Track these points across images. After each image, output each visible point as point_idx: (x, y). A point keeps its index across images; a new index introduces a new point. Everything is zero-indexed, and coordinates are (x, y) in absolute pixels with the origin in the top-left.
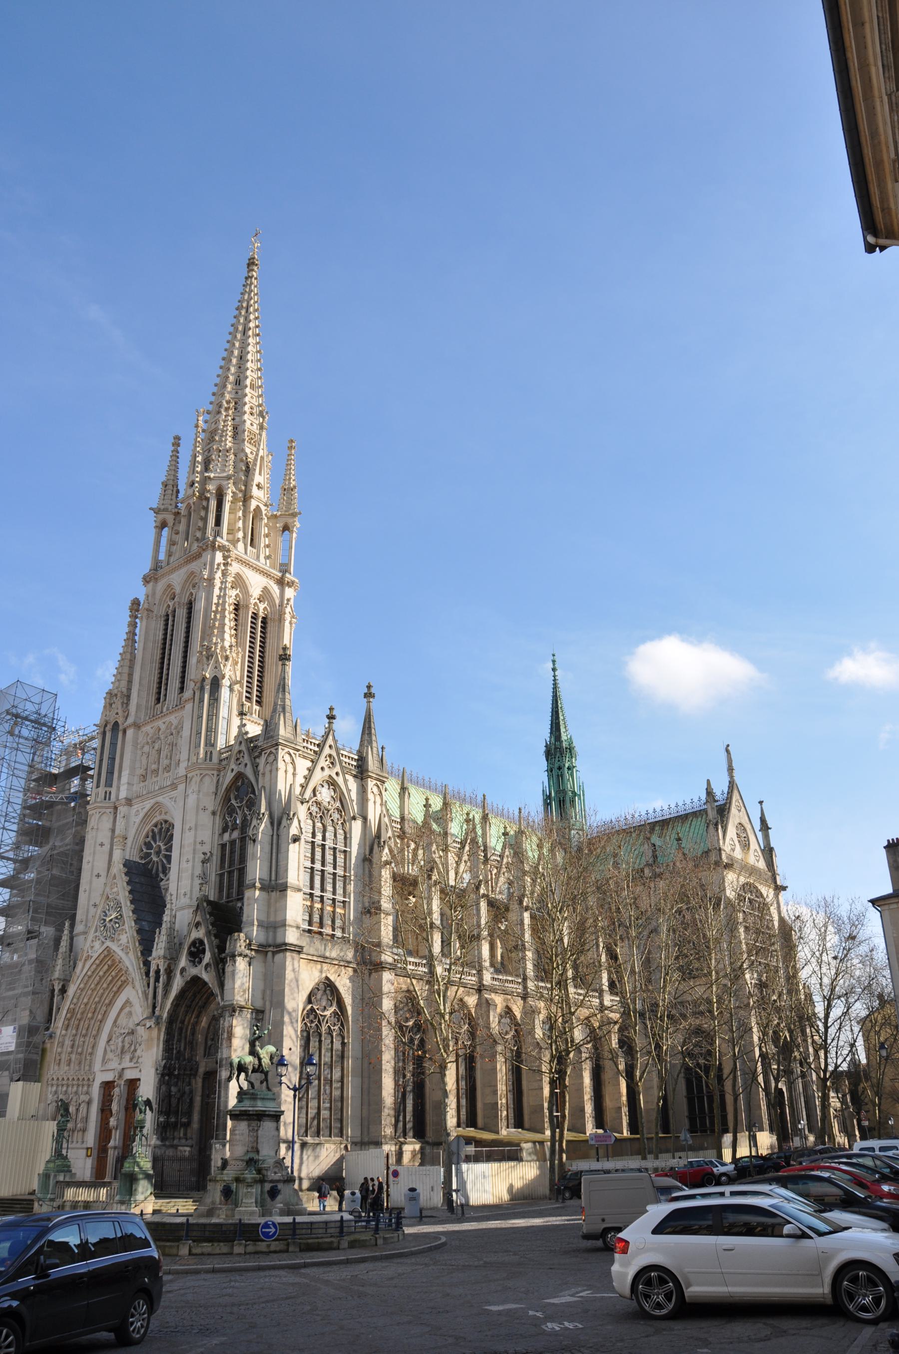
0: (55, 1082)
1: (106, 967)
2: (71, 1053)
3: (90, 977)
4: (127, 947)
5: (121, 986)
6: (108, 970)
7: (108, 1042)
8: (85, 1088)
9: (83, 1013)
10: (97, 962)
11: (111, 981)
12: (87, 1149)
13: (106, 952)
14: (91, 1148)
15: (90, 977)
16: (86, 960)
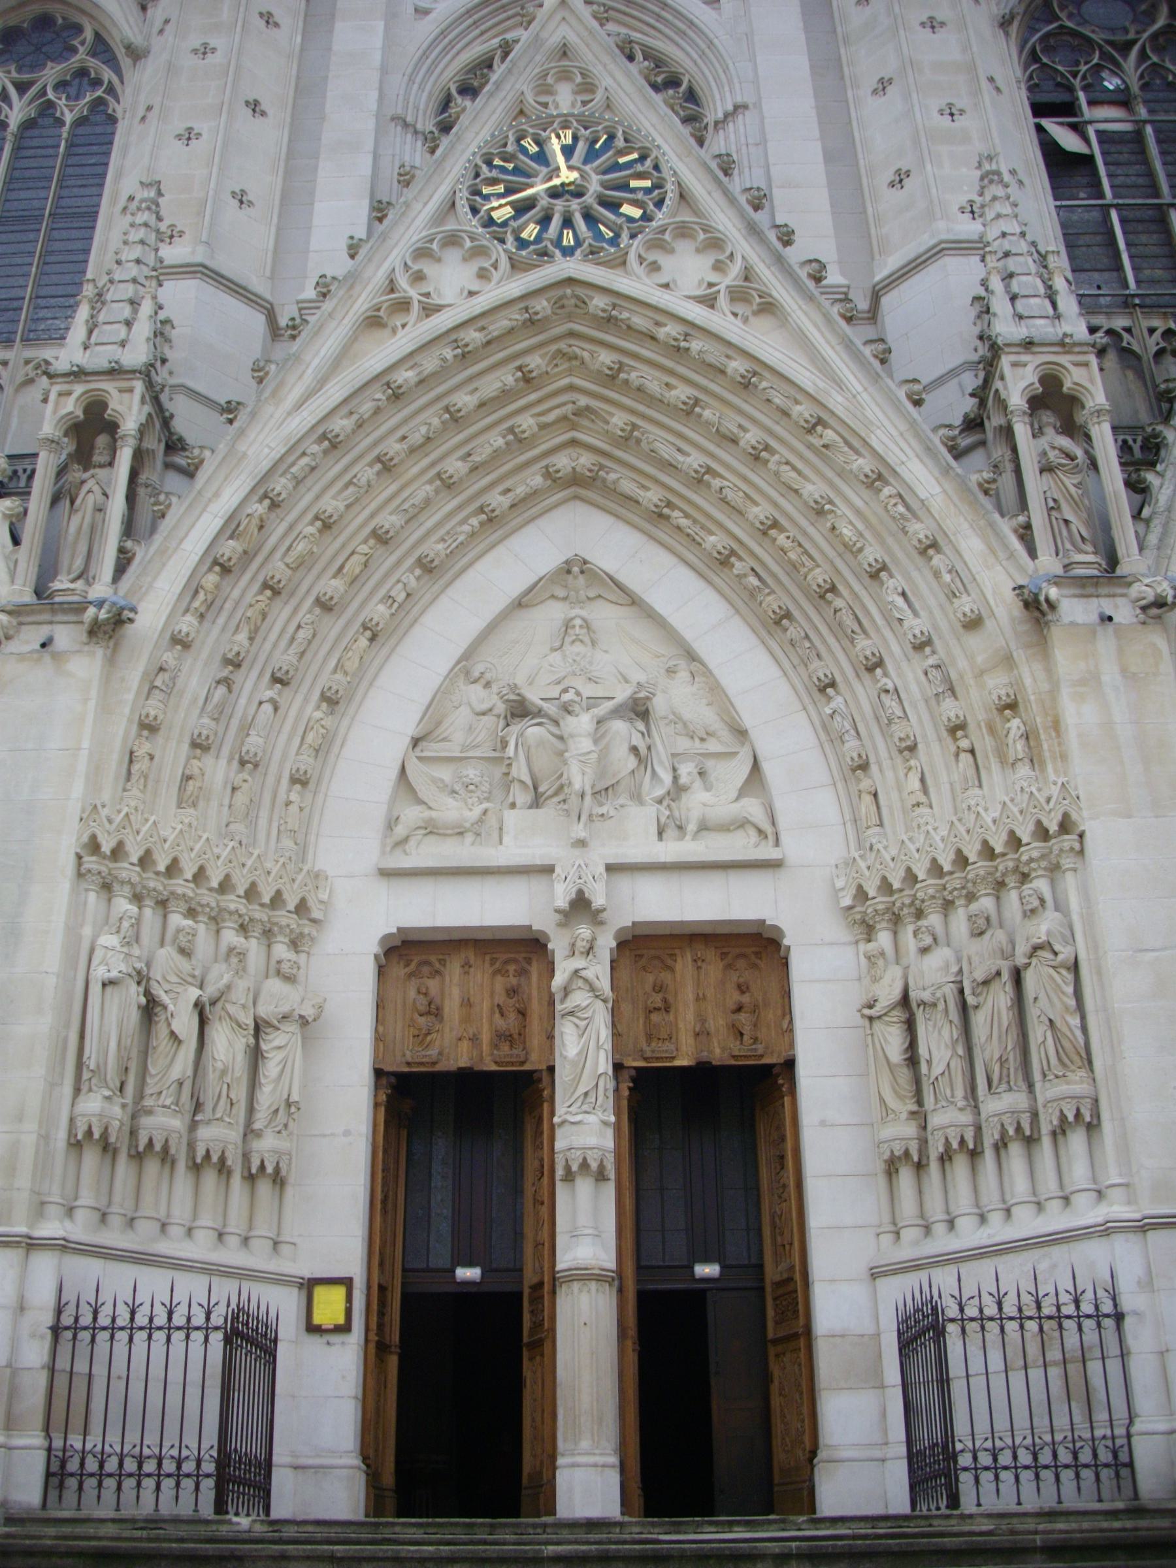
0: (127, 870)
1: (508, 377)
2: (199, 746)
3: (397, 396)
4: (738, 295)
5: (534, 494)
6: (505, 396)
7: (416, 742)
8: (281, 950)
9: (301, 565)
10: (473, 336)
11: (497, 454)
12: (309, 1286)
13: (542, 306)
14: (347, 1282)
15: (397, 396)
16: (373, 322)
